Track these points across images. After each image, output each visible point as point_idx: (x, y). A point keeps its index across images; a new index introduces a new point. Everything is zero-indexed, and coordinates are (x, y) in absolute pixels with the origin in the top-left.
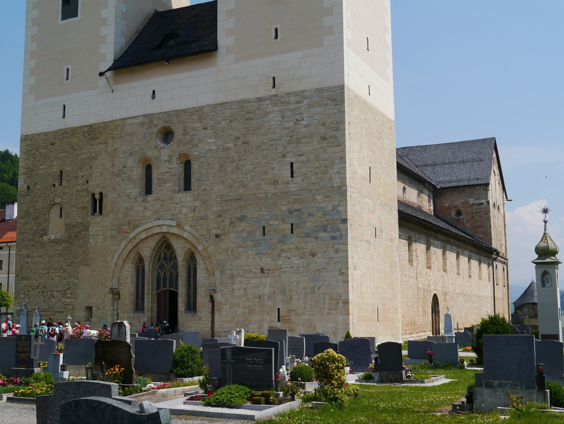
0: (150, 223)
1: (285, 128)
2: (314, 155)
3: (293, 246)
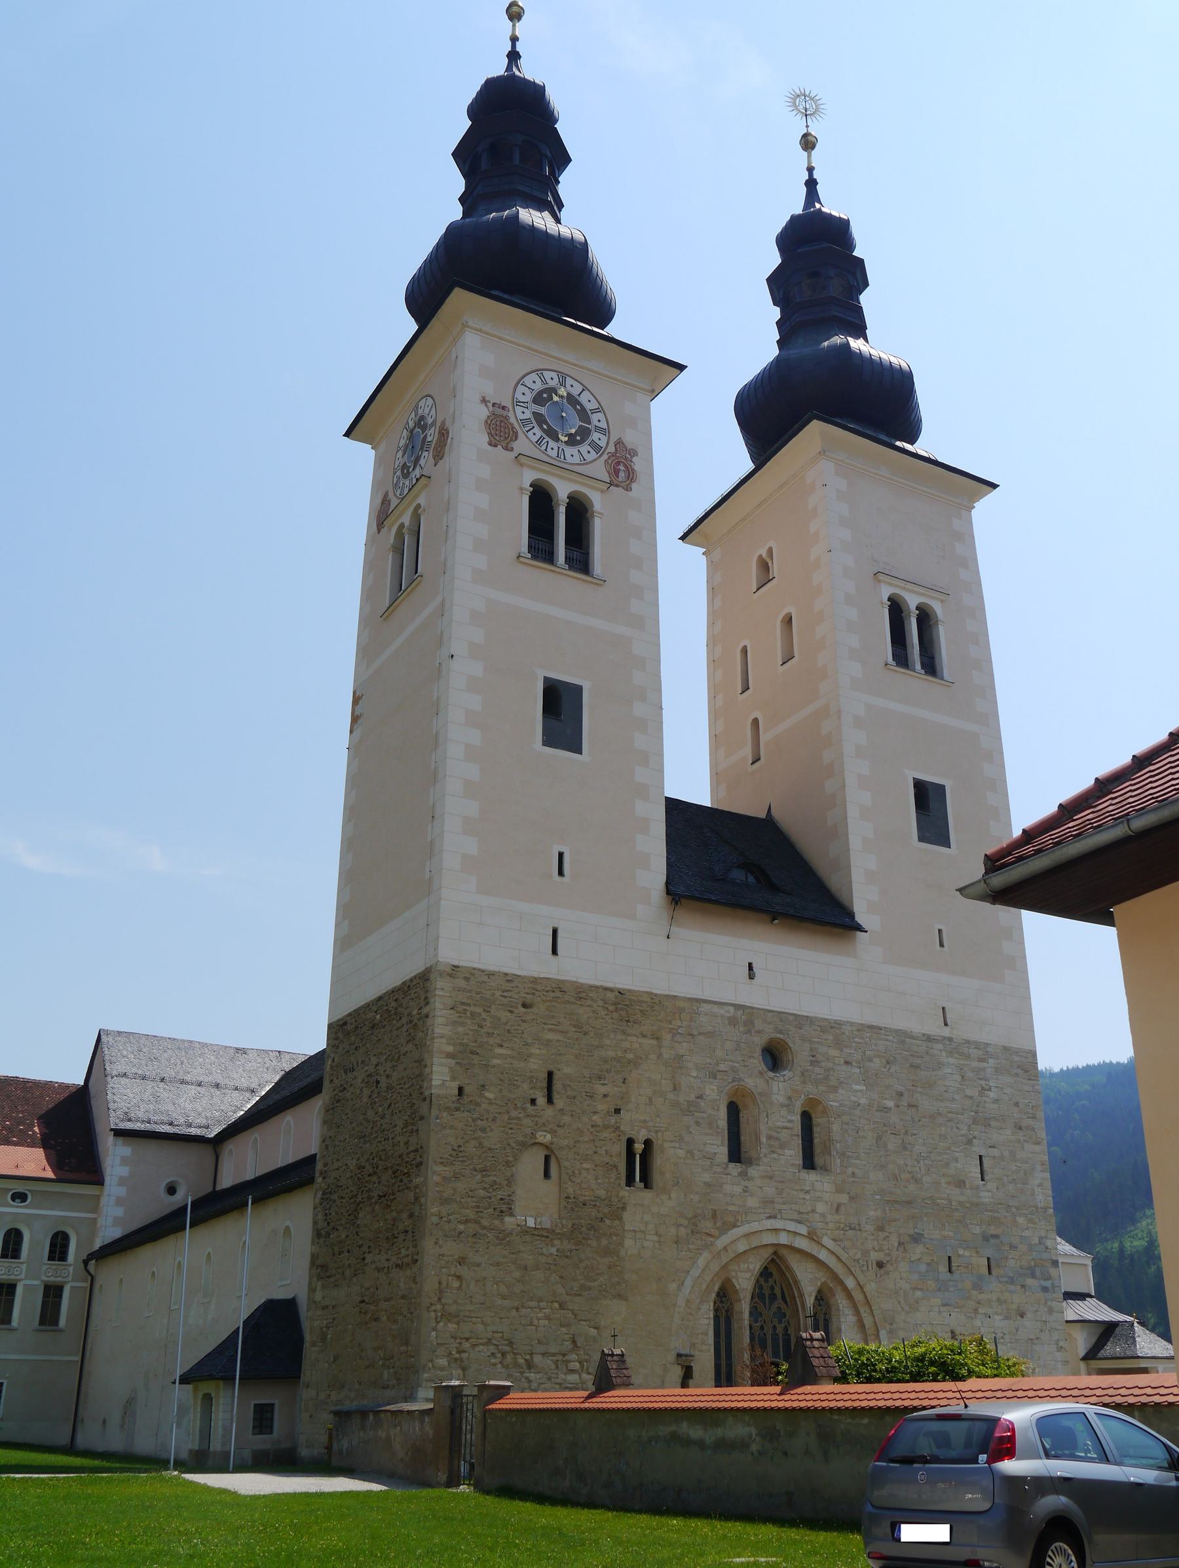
0: (757, 1223)
1: (967, 1096)
2: (1009, 1150)
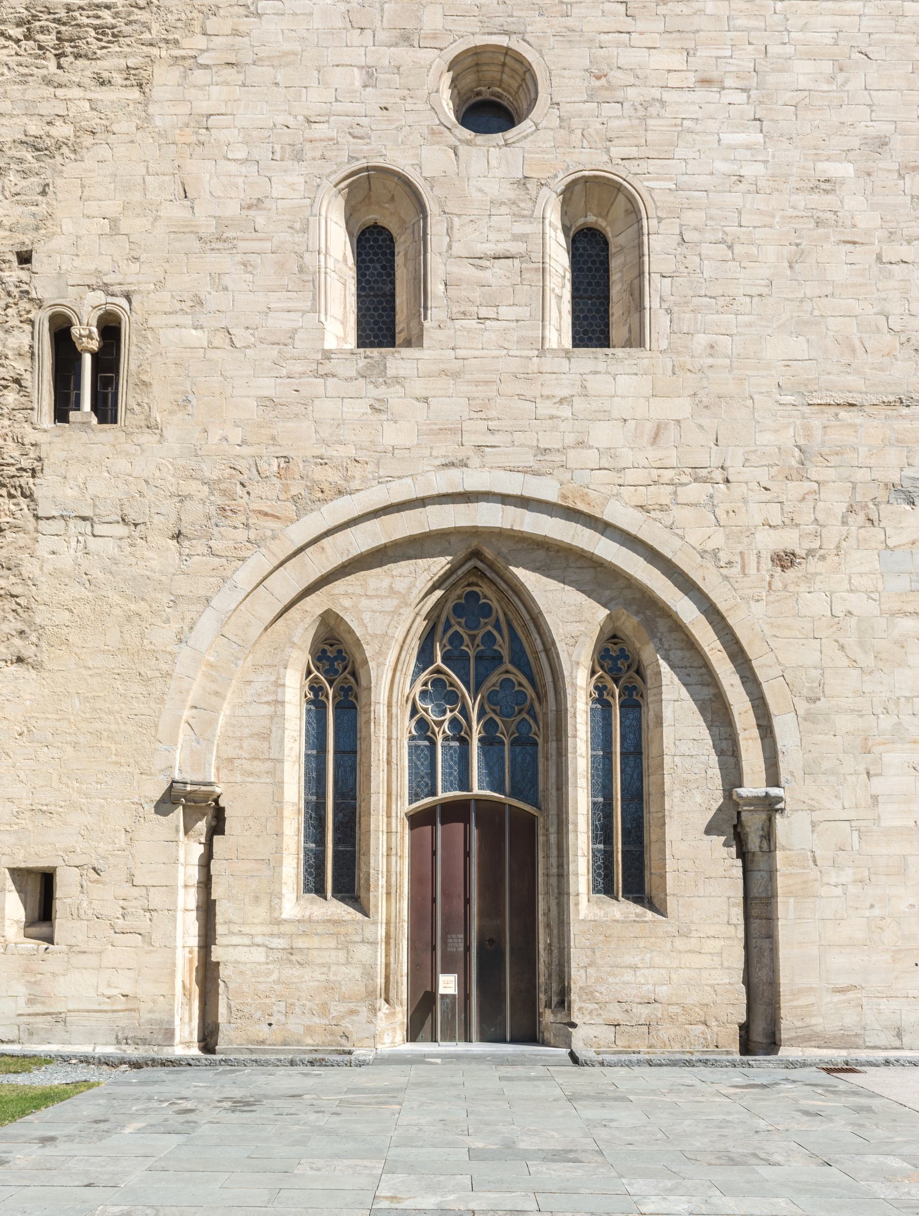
0: (409, 480)
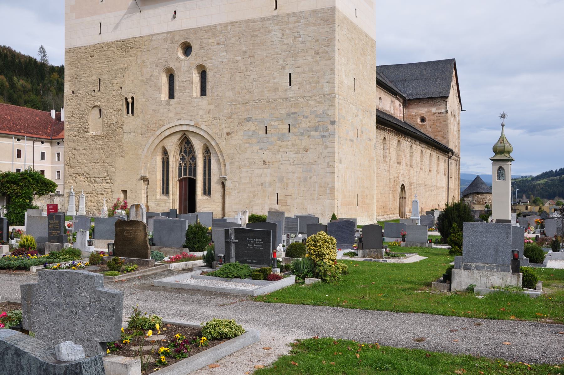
3: (290, 143)
